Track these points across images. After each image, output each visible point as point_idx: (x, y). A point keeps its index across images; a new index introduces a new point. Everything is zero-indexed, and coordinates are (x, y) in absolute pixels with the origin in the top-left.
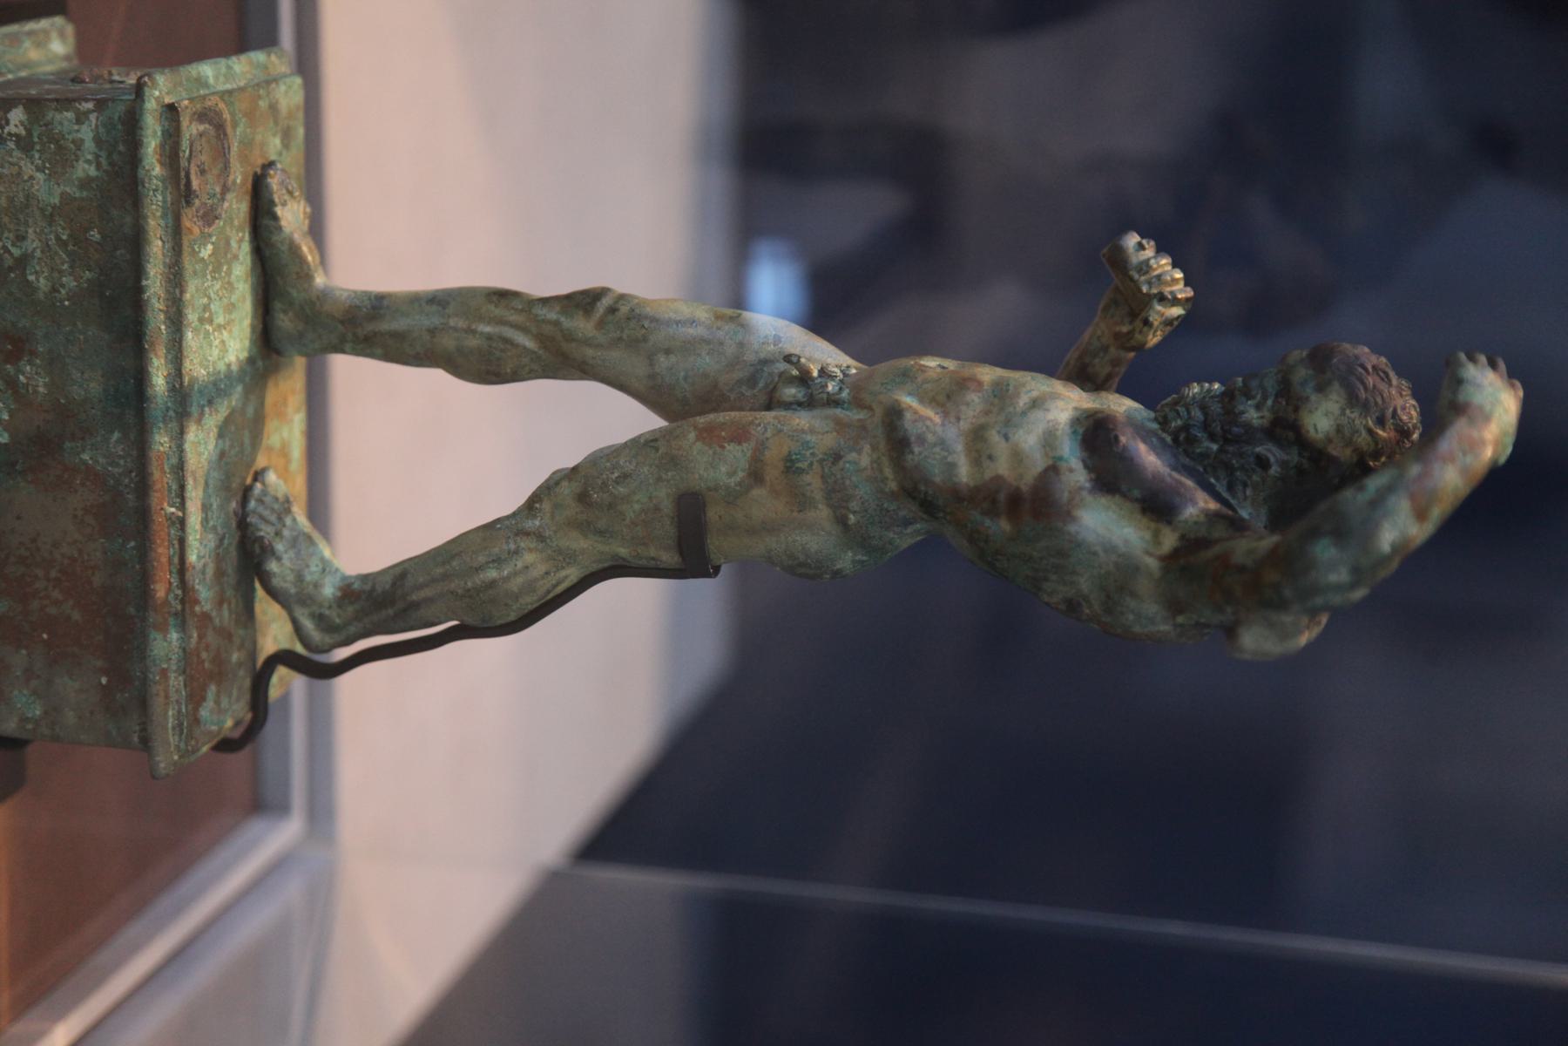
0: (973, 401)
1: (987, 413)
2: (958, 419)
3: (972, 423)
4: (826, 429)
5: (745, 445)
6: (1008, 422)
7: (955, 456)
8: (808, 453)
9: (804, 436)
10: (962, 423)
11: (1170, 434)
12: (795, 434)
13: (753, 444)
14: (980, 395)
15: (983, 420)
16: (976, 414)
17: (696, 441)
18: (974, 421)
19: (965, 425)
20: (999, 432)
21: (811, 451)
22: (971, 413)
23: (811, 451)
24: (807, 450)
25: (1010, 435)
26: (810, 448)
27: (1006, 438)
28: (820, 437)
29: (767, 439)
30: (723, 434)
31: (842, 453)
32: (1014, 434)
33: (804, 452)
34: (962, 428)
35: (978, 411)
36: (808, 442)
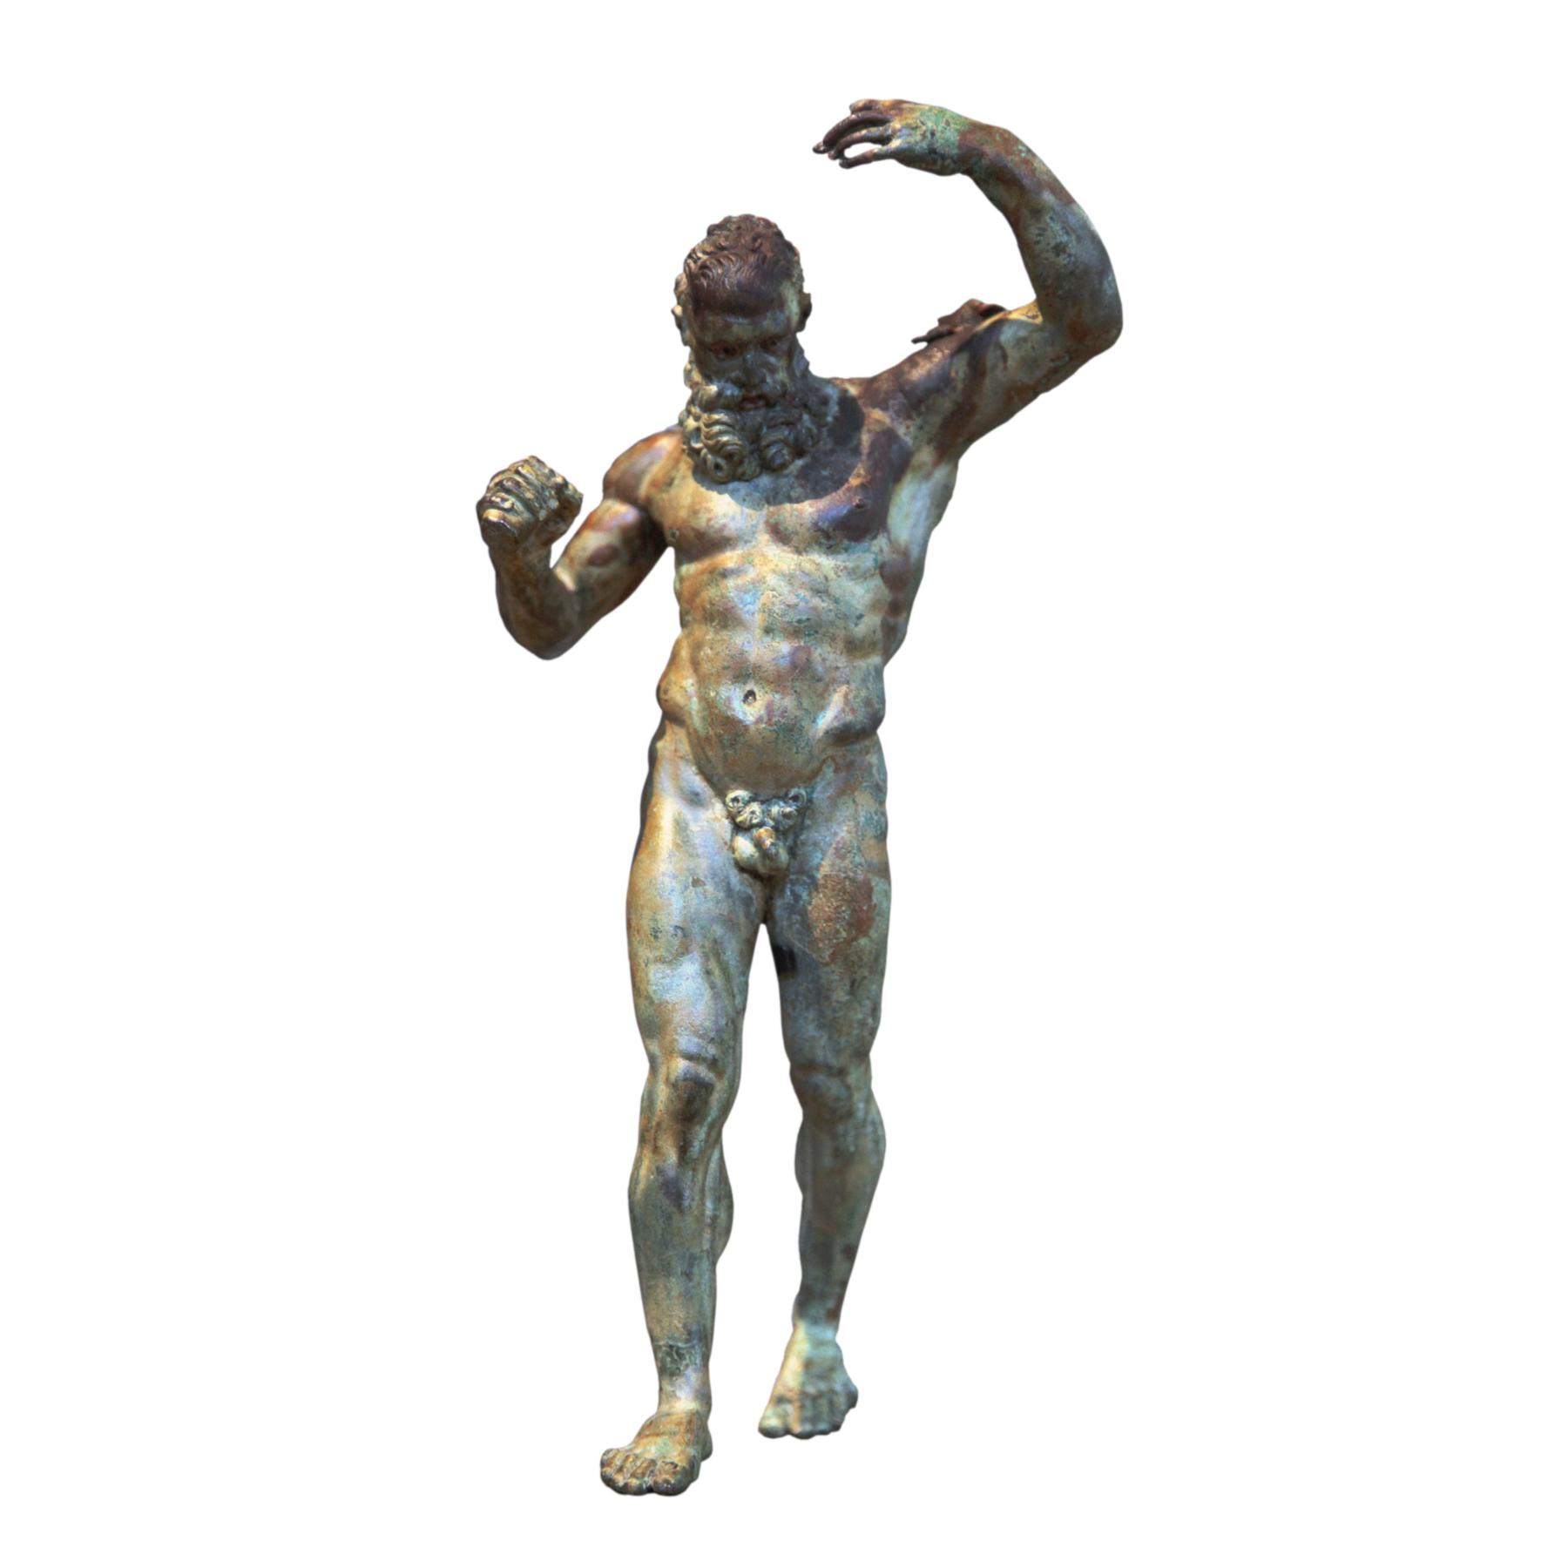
0: (820, 655)
1: (833, 639)
2: (837, 668)
3: (841, 653)
4: (851, 802)
5: (873, 884)
6: (845, 617)
7: (870, 668)
8: (876, 818)
9: (861, 824)
10: (840, 665)
11: (793, 461)
12: (860, 833)
13: (870, 876)
14: (812, 649)
15: (840, 645)
16: (833, 650)
17: (869, 937)
18: (838, 652)
19: (842, 662)
20: (856, 625)
21: (874, 815)
22: (832, 656)
23: (874, 815)
24: (873, 819)
25: (858, 613)
26: (871, 816)
27: (860, 617)
28: (860, 808)
29: (866, 862)
30: (865, 908)
31: (875, 783)
32: (856, 609)
33: (875, 822)
34: (845, 664)
35: (829, 649)
36: (866, 819)
